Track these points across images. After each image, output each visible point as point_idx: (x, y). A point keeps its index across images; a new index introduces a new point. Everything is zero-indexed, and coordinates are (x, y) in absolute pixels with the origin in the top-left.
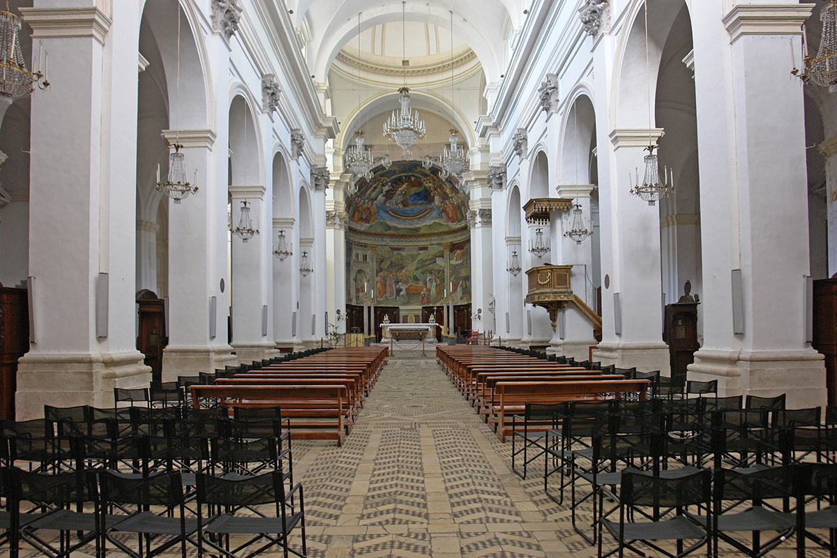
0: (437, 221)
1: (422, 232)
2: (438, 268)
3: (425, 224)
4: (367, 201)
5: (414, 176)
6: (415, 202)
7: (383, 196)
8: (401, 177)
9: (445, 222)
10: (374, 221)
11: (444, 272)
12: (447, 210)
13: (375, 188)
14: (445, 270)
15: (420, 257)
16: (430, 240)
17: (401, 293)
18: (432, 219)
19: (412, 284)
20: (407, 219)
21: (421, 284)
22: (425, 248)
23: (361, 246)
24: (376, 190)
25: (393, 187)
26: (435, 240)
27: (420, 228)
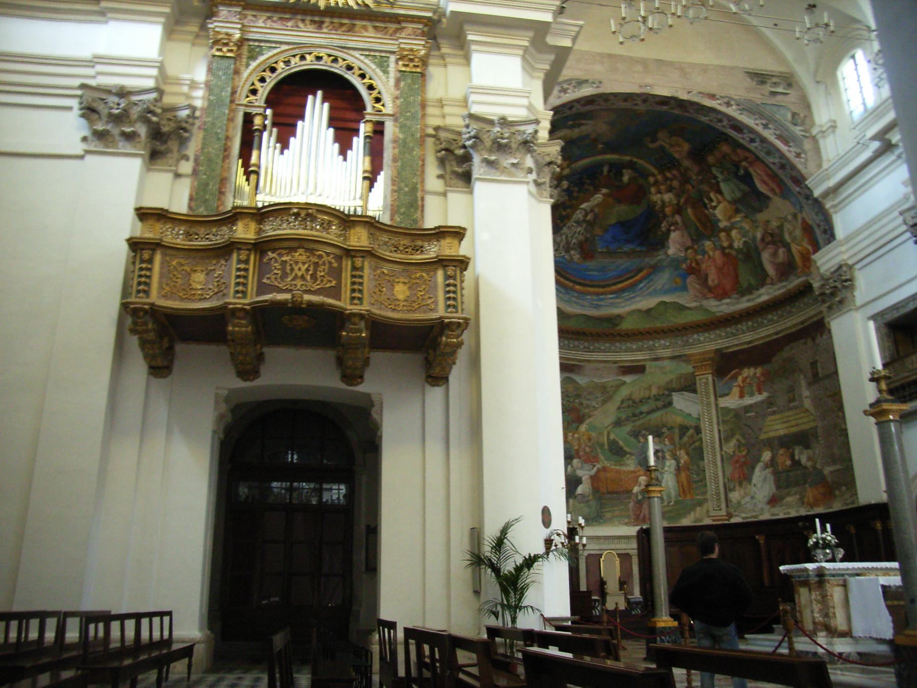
0: (667, 299)
1: (626, 326)
2: (679, 420)
3: (634, 307)
8: (601, 165)
11: (698, 430)
12: (703, 266)
14: (705, 426)
15: (624, 392)
16: (650, 349)
17: (580, 490)
18: (655, 293)
19: (607, 464)
20: (588, 293)
21: (631, 465)
22: (637, 369)
26: (665, 348)
27: (620, 317)
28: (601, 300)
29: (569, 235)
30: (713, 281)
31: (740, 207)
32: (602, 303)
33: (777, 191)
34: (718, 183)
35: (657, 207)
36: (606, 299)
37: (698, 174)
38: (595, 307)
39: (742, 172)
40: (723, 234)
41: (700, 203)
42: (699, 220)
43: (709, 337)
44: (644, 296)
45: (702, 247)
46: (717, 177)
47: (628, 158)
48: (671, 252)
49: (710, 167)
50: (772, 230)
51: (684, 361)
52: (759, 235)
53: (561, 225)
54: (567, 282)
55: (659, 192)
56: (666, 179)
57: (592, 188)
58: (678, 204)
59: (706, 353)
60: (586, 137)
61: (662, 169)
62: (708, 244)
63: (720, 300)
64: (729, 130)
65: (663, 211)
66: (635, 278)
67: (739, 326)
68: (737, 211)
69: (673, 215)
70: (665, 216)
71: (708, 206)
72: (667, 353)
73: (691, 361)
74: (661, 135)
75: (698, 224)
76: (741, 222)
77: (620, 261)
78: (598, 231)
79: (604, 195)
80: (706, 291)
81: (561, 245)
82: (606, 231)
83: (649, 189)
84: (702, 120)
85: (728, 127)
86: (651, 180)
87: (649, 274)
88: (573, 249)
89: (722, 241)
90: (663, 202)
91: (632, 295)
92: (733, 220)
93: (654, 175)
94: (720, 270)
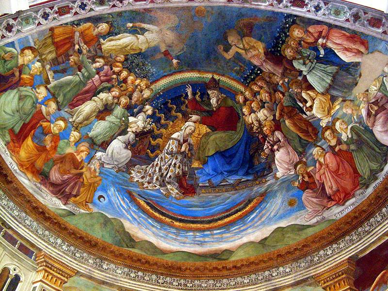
0: (283, 224)
3: (245, 240)
4: (75, 135)
5: (215, 84)
6: (216, 180)
7: (128, 145)
8: (182, 85)
9: (316, 213)
10: (85, 204)
12: (317, 177)
13: (105, 111)
18: (270, 220)
20: (191, 230)
23: (13, 241)
24: (110, 118)
25: (157, 121)
27: (229, 252)
28: (207, 236)
29: (164, 167)
30: (331, 188)
31: (335, 93)
32: (207, 239)
33: (362, 49)
34: (305, 77)
35: (255, 128)
36: (212, 235)
37: (283, 75)
38: (199, 244)
39: (322, 52)
40: (328, 133)
41: (295, 110)
42: (300, 129)
43: (338, 248)
44: (258, 226)
45: (311, 158)
46: (302, 71)
47: (210, 76)
48: (279, 175)
49: (290, 62)
50: (374, 98)
51: (310, 285)
52: (364, 113)
53: (151, 155)
54: (164, 218)
55: (252, 111)
56: (255, 94)
57: (180, 115)
58: (274, 120)
59: (337, 266)
60: (155, 49)
61: (247, 81)
62: (315, 151)
63: (343, 205)
64: (292, 8)
65: (261, 132)
66: (245, 210)
67: (372, 220)
68: (333, 99)
69: (273, 132)
70: (265, 137)
71: (304, 109)
72: (290, 280)
73: (319, 282)
74: (232, 39)
75: (301, 135)
76: (341, 108)
77: (227, 194)
78: (196, 165)
79: (195, 122)
80: (325, 201)
81: (155, 178)
82: (205, 163)
83: (241, 110)
84: (262, 7)
85: (289, 5)
86: (241, 99)
87: (260, 203)
88: (169, 183)
89: (329, 141)
90: (259, 121)
91: (242, 228)
92: (333, 112)
93: (242, 92)
94: (336, 173)
